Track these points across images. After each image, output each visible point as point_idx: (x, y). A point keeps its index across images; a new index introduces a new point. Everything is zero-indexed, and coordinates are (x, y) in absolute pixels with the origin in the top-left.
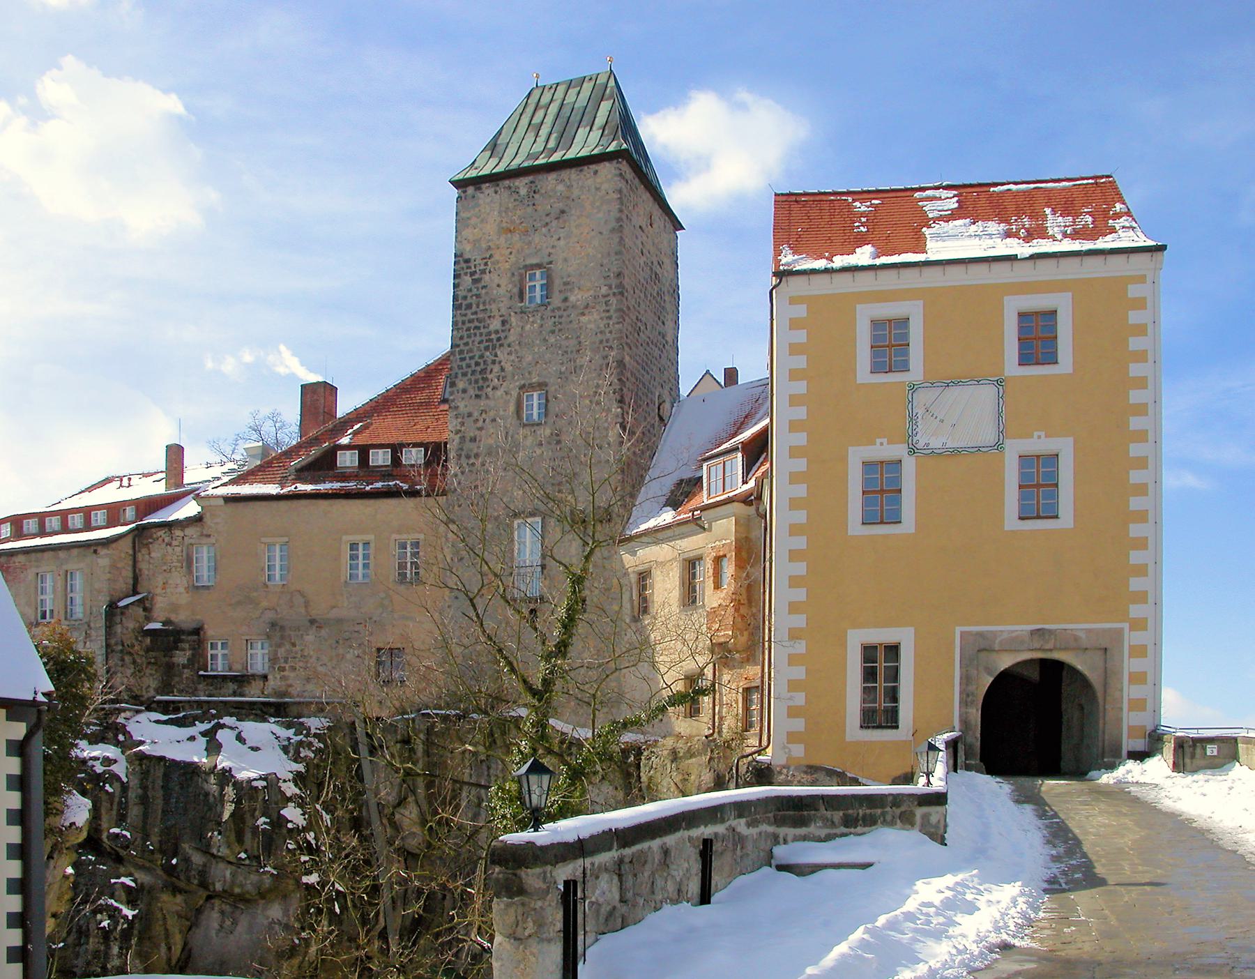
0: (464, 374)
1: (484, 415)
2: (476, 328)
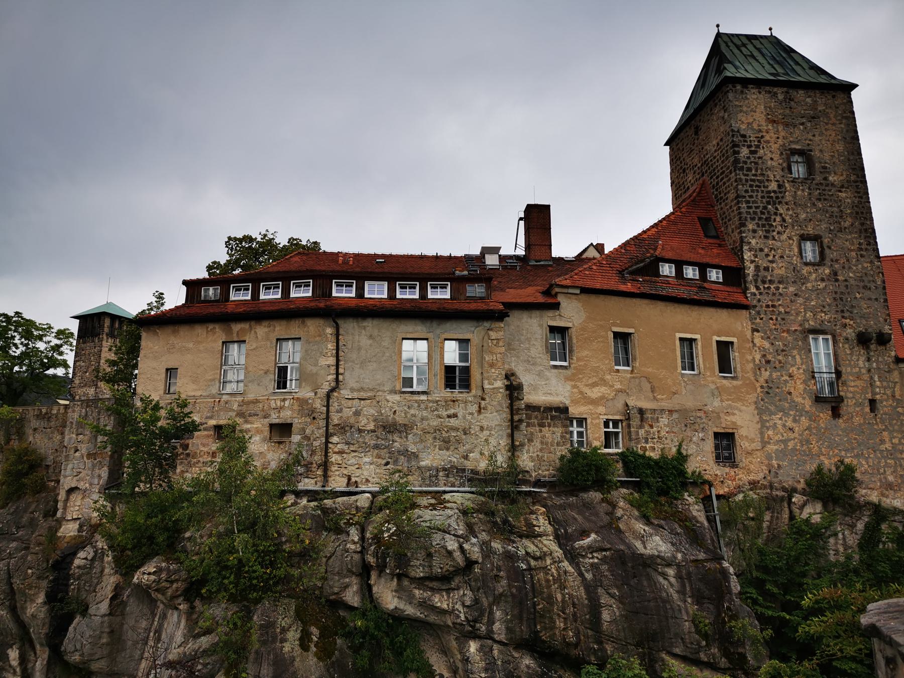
0: (753, 219)
1: (773, 252)
2: (757, 186)
